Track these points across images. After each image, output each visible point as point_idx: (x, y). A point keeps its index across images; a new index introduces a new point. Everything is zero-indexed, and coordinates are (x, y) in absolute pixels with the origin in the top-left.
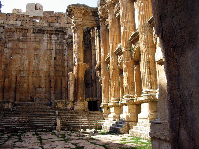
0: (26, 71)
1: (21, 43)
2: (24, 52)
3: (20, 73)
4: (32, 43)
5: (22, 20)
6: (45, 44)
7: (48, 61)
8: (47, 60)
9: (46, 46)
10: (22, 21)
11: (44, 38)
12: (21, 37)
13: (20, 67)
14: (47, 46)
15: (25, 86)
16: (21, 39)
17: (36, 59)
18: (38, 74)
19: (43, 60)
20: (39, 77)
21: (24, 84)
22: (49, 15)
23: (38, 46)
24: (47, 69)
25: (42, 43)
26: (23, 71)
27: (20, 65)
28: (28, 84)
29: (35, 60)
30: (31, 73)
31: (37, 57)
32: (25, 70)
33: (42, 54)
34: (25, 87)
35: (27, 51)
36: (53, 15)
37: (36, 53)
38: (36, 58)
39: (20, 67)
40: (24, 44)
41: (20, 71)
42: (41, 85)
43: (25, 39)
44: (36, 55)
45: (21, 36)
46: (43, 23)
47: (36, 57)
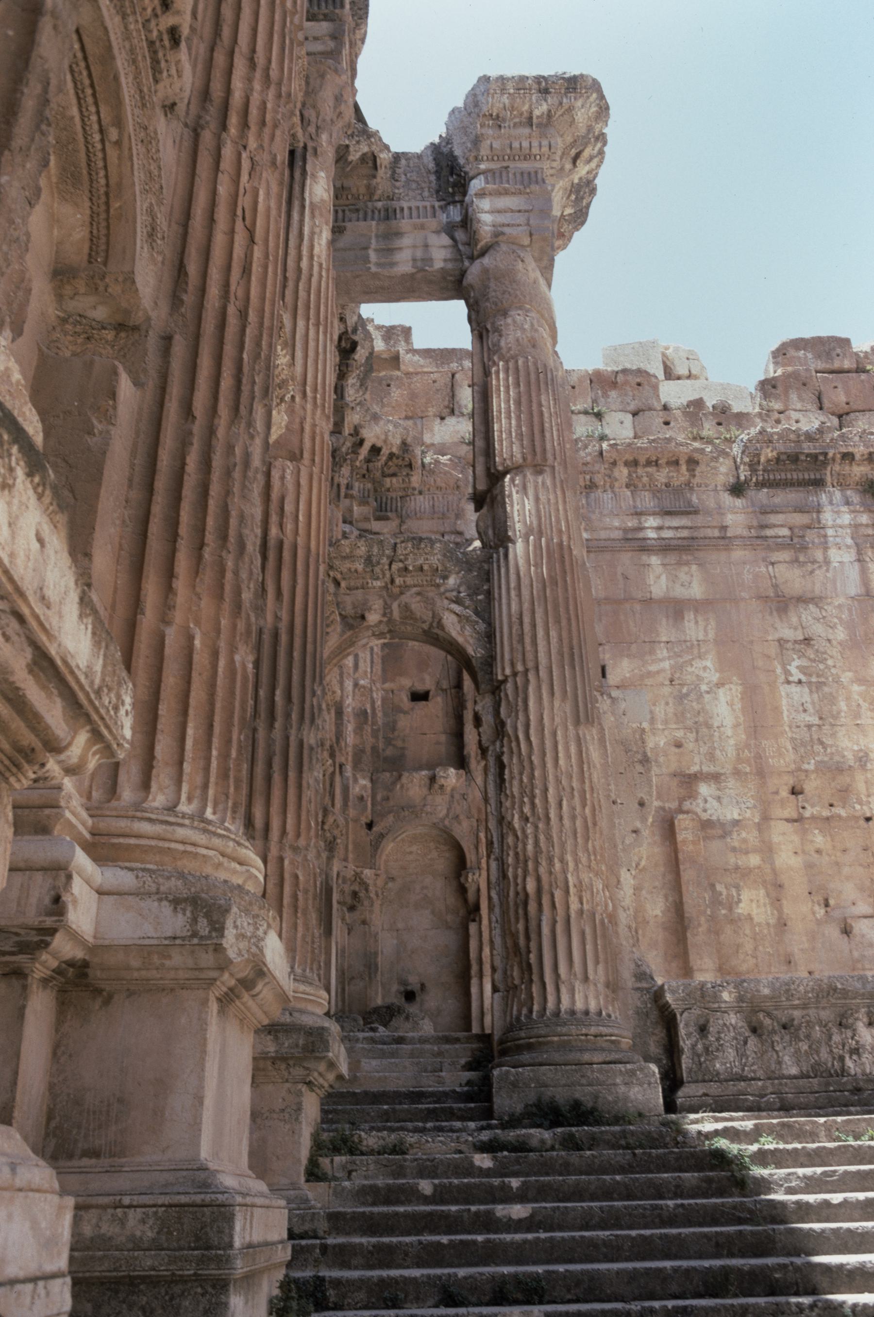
0: (737, 773)
2: (694, 628)
3: (692, 795)
4: (738, 554)
5: (632, 407)
6: (841, 556)
9: (853, 573)
10: (635, 414)
11: (827, 517)
12: (652, 522)
13: (679, 745)
15: (752, 903)
16: (652, 534)
17: (796, 675)
18: (844, 803)
20: (856, 818)
21: (738, 887)
22: (821, 365)
23: (792, 578)
25: (819, 555)
26: (716, 777)
27: (679, 734)
28: (776, 889)
29: (794, 689)
30: (784, 793)
31: (804, 662)
32: (728, 769)
33: (841, 634)
34: (750, 918)
35: (713, 623)
36: (847, 364)
37: (787, 633)
38: (793, 669)
39: (679, 745)
40: (686, 569)
41: (689, 781)
43: (685, 533)
44: (789, 645)
45: (654, 514)
46: (794, 415)
47: (796, 663)
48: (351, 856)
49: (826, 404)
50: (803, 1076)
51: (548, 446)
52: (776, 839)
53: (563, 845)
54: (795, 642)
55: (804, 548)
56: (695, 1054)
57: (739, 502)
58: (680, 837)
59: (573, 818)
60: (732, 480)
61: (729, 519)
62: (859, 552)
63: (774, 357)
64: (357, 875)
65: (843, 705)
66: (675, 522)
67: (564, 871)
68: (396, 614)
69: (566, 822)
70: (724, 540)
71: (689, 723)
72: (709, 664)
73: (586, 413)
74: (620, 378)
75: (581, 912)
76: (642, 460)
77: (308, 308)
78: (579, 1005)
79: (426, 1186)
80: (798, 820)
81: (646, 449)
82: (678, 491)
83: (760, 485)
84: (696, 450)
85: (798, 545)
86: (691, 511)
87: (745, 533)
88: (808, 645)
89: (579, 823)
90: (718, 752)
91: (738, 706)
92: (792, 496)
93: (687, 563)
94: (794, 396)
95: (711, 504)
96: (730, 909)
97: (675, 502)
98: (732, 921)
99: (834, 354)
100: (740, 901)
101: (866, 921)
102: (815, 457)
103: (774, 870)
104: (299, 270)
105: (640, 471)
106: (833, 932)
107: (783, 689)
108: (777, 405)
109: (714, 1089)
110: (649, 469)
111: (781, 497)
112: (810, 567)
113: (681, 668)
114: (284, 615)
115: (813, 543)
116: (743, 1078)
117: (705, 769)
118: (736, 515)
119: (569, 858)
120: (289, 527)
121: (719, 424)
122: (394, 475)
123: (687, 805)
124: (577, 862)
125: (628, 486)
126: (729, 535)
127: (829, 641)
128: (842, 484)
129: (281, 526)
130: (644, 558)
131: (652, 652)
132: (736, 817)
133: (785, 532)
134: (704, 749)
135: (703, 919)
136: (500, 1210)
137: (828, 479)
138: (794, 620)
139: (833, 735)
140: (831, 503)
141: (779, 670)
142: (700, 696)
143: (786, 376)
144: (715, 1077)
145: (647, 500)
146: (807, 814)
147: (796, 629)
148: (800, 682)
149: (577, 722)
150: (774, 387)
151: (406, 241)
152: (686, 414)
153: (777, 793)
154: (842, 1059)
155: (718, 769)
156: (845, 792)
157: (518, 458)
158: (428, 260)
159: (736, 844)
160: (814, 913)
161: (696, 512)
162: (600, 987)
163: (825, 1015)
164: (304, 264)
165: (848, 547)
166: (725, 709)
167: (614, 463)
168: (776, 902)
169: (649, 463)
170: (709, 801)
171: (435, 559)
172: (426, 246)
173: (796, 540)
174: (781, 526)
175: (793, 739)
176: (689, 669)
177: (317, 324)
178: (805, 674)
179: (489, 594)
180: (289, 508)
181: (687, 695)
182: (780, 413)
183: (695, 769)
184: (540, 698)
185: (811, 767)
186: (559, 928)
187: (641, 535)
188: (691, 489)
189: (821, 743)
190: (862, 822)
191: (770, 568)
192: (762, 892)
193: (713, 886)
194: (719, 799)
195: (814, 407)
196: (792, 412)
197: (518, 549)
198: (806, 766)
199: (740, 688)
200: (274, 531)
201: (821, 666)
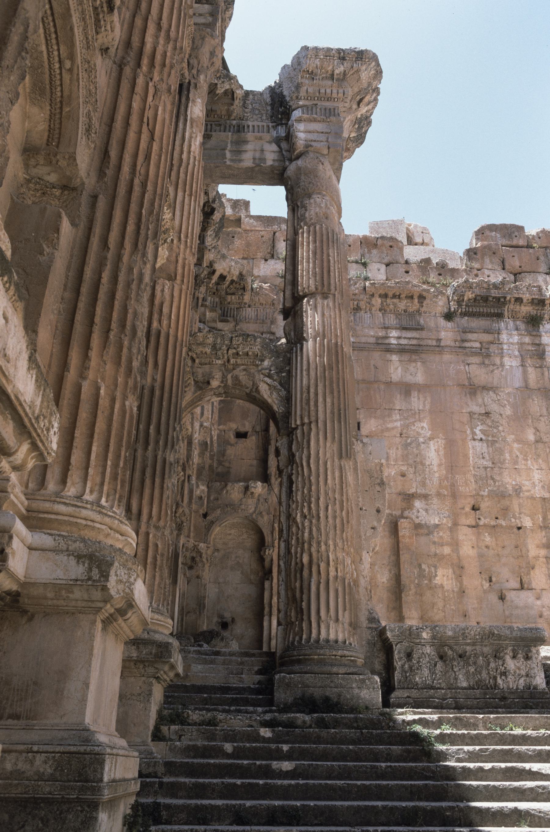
0: (439, 494)
1: (395, 358)
2: (417, 402)
3: (410, 507)
4: (447, 357)
5: (386, 261)
6: (511, 362)
7: (540, 445)
8: (537, 442)
9: (518, 373)
10: (387, 265)
11: (504, 337)
12: (394, 333)
13: (403, 475)
14: (525, 372)
15: (444, 577)
16: (394, 341)
17: (479, 435)
18: (505, 516)
19: (518, 441)
21: (435, 567)
22: (505, 242)
23: (479, 374)
24: (543, 487)
25: (498, 361)
26: (425, 497)
27: (404, 468)
28: (459, 569)
29: (477, 443)
30: (468, 509)
31: (484, 427)
32: (433, 492)
33: (508, 411)
34: (442, 586)
35: (429, 399)
36: (521, 242)
37: (475, 409)
38: (477, 431)
39: (403, 475)
40: (414, 364)
41: (408, 498)
42: (528, 574)
43: (414, 342)
46: (487, 272)
48: (192, 534)
49: (507, 267)
50: (470, 688)
51: (332, 282)
52: (461, 537)
53: (327, 535)
54: (480, 414)
55: (488, 356)
56: (404, 671)
57: (449, 325)
58: (401, 534)
59: (335, 517)
60: (446, 310)
61: (443, 335)
62: (523, 360)
63: (476, 235)
64: (195, 546)
65: (507, 456)
66: (409, 334)
67: (327, 551)
68: (230, 382)
69: (330, 519)
70: (439, 348)
71: (411, 461)
72: (425, 425)
73: (357, 262)
74: (380, 242)
75: (336, 577)
76: (390, 294)
77: (185, 184)
78: (332, 637)
79: (228, 747)
80: (476, 526)
81: (393, 287)
82: (411, 315)
83: (464, 314)
84: (424, 290)
85: (484, 353)
86: (420, 328)
87: (452, 344)
88: (488, 416)
89: (338, 520)
90: (428, 481)
91: (442, 453)
92: (482, 323)
93: (415, 361)
94: (487, 260)
95: (432, 324)
96: (430, 580)
97: (410, 323)
98: (430, 588)
99: (514, 235)
100: (436, 575)
101: (514, 592)
102: (498, 299)
103: (459, 557)
104: (181, 160)
105: (388, 301)
106: (493, 598)
107: (471, 444)
108: (476, 265)
109: (414, 693)
110: (395, 300)
111: (475, 323)
112: (491, 368)
113: (407, 426)
114: (159, 378)
115: (494, 352)
116: (432, 688)
117: (419, 491)
118: (447, 333)
119: (331, 542)
120: (165, 323)
121: (440, 275)
122: (233, 294)
123: (406, 513)
124: (335, 545)
125: (380, 310)
126: (442, 344)
127: (501, 415)
128: (514, 317)
129: (160, 321)
130: (388, 356)
131: (390, 416)
132: (437, 522)
133: (478, 345)
134: (419, 479)
135: (412, 586)
136: (275, 765)
137: (506, 313)
138: (480, 400)
139: (500, 474)
140: (507, 329)
141: (468, 432)
142: (419, 445)
143: (483, 247)
144: (415, 686)
145: (392, 320)
146: (481, 523)
147: (480, 406)
148: (481, 440)
149: (341, 457)
150: (475, 254)
151: (249, 147)
152: (419, 267)
153: (463, 508)
154: (495, 678)
155: (427, 491)
156: (506, 510)
157: (313, 288)
158: (263, 160)
159: (436, 540)
160: (482, 586)
161: (422, 329)
162: (346, 626)
163: (486, 650)
164: (184, 156)
165: (516, 357)
166: (433, 454)
167: (373, 295)
168: (459, 578)
169: (394, 296)
170: (420, 511)
171: (257, 349)
172: (262, 151)
173: (483, 350)
174: (475, 341)
175: (475, 476)
176: (413, 428)
177: (191, 195)
178: (485, 435)
179: (289, 372)
180: (165, 310)
181: (410, 444)
182: (478, 270)
183: (413, 490)
184: (318, 440)
185: (486, 494)
186: (322, 587)
187: (387, 341)
188: (420, 314)
189: (493, 479)
190: (515, 530)
191: (467, 367)
192: (451, 571)
193: (420, 566)
194: (426, 510)
195: (499, 268)
196: (486, 271)
197: (309, 345)
198: (482, 493)
199: (443, 442)
200: (155, 324)
201: (495, 431)
